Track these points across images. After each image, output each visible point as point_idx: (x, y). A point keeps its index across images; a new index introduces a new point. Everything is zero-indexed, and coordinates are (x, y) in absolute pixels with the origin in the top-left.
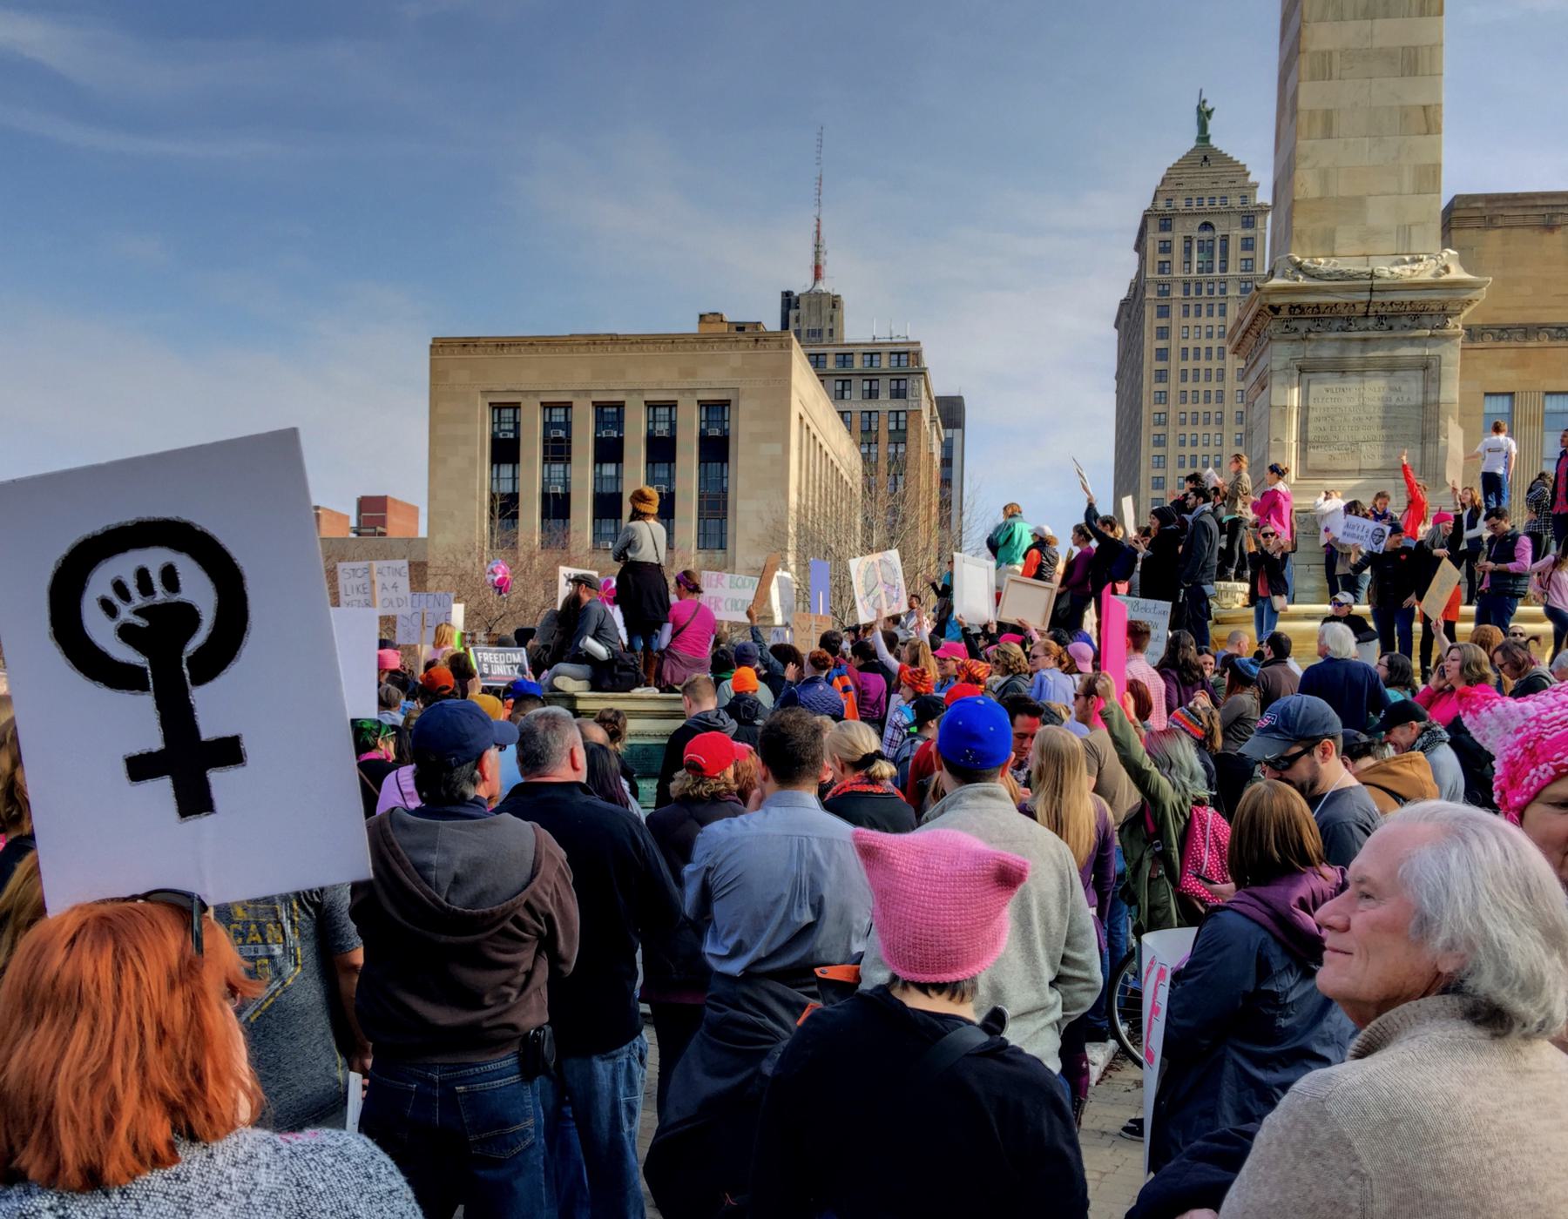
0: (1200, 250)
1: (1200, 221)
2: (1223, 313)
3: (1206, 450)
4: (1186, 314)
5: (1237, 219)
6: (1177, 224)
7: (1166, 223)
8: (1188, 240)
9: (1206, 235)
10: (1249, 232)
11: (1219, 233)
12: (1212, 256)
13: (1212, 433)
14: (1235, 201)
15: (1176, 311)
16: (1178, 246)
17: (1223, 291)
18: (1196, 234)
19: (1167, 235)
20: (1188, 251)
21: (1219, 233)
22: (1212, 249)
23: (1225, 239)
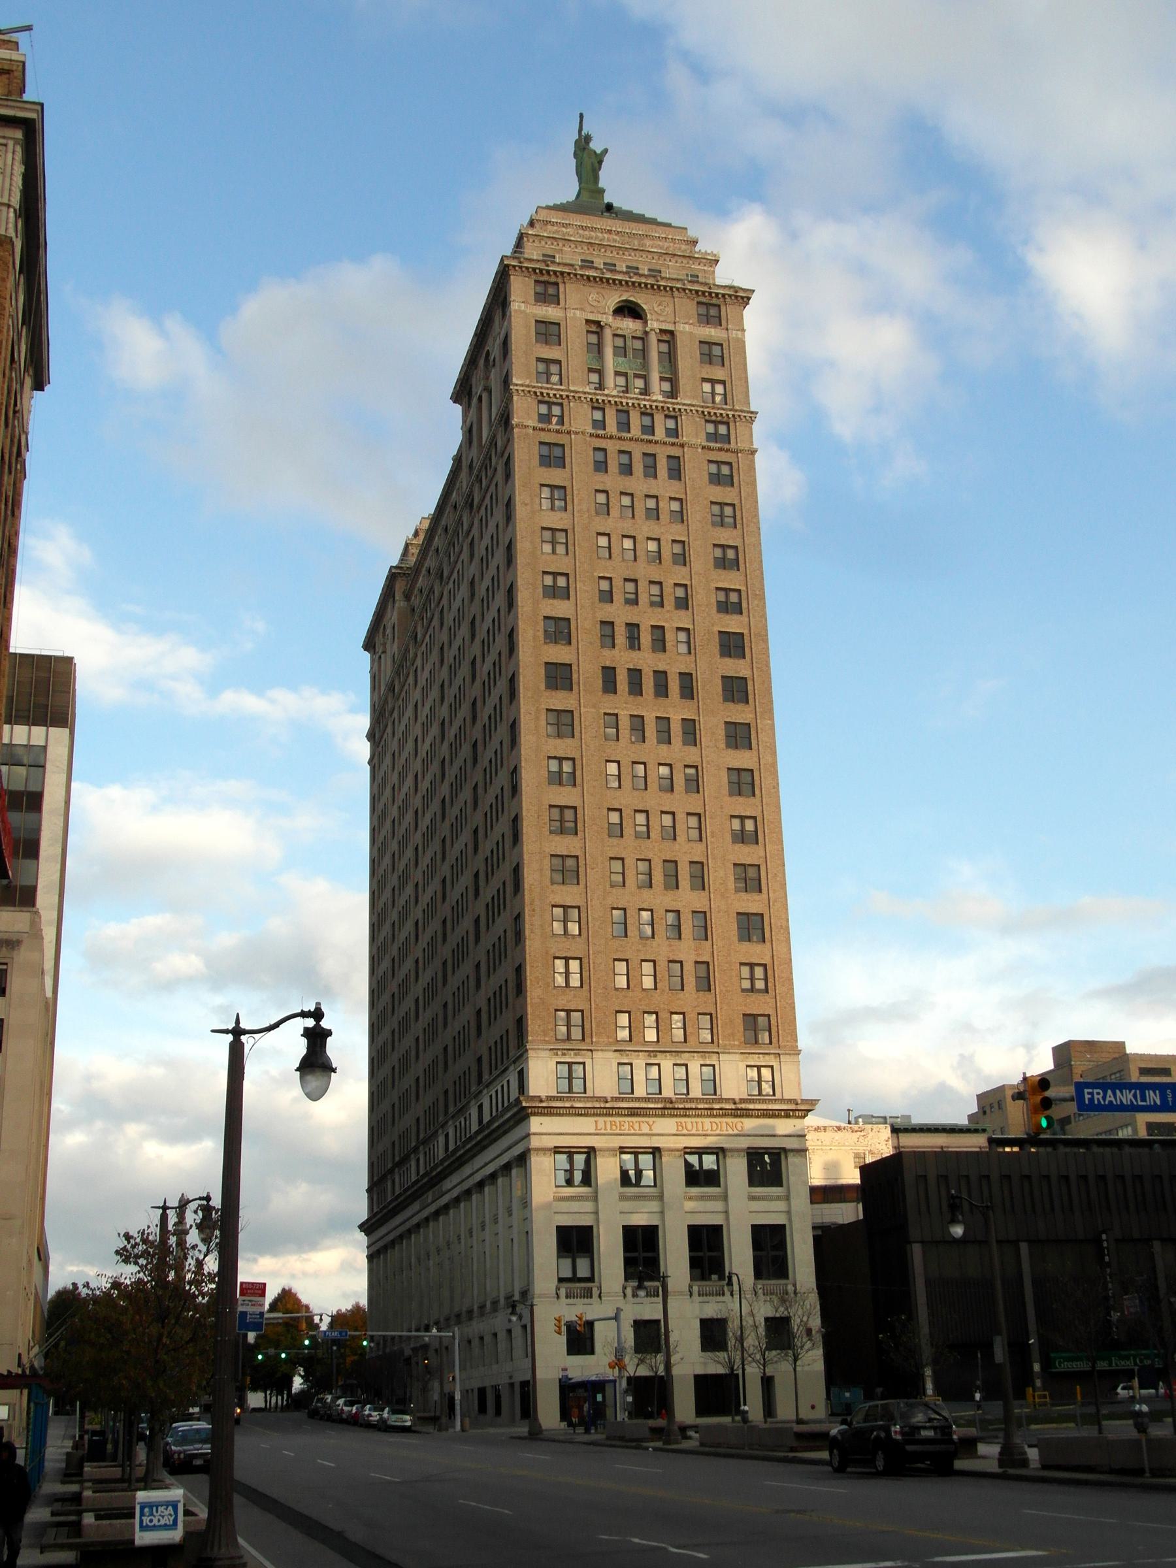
0: (621, 351)
1: (614, 298)
2: (676, 472)
4: (601, 466)
5: (688, 307)
6: (571, 293)
7: (548, 287)
8: (596, 328)
9: (629, 325)
10: (712, 333)
12: (645, 364)
17: (674, 433)
18: (607, 318)
19: (550, 312)
21: (653, 324)
22: (644, 353)
23: (669, 337)
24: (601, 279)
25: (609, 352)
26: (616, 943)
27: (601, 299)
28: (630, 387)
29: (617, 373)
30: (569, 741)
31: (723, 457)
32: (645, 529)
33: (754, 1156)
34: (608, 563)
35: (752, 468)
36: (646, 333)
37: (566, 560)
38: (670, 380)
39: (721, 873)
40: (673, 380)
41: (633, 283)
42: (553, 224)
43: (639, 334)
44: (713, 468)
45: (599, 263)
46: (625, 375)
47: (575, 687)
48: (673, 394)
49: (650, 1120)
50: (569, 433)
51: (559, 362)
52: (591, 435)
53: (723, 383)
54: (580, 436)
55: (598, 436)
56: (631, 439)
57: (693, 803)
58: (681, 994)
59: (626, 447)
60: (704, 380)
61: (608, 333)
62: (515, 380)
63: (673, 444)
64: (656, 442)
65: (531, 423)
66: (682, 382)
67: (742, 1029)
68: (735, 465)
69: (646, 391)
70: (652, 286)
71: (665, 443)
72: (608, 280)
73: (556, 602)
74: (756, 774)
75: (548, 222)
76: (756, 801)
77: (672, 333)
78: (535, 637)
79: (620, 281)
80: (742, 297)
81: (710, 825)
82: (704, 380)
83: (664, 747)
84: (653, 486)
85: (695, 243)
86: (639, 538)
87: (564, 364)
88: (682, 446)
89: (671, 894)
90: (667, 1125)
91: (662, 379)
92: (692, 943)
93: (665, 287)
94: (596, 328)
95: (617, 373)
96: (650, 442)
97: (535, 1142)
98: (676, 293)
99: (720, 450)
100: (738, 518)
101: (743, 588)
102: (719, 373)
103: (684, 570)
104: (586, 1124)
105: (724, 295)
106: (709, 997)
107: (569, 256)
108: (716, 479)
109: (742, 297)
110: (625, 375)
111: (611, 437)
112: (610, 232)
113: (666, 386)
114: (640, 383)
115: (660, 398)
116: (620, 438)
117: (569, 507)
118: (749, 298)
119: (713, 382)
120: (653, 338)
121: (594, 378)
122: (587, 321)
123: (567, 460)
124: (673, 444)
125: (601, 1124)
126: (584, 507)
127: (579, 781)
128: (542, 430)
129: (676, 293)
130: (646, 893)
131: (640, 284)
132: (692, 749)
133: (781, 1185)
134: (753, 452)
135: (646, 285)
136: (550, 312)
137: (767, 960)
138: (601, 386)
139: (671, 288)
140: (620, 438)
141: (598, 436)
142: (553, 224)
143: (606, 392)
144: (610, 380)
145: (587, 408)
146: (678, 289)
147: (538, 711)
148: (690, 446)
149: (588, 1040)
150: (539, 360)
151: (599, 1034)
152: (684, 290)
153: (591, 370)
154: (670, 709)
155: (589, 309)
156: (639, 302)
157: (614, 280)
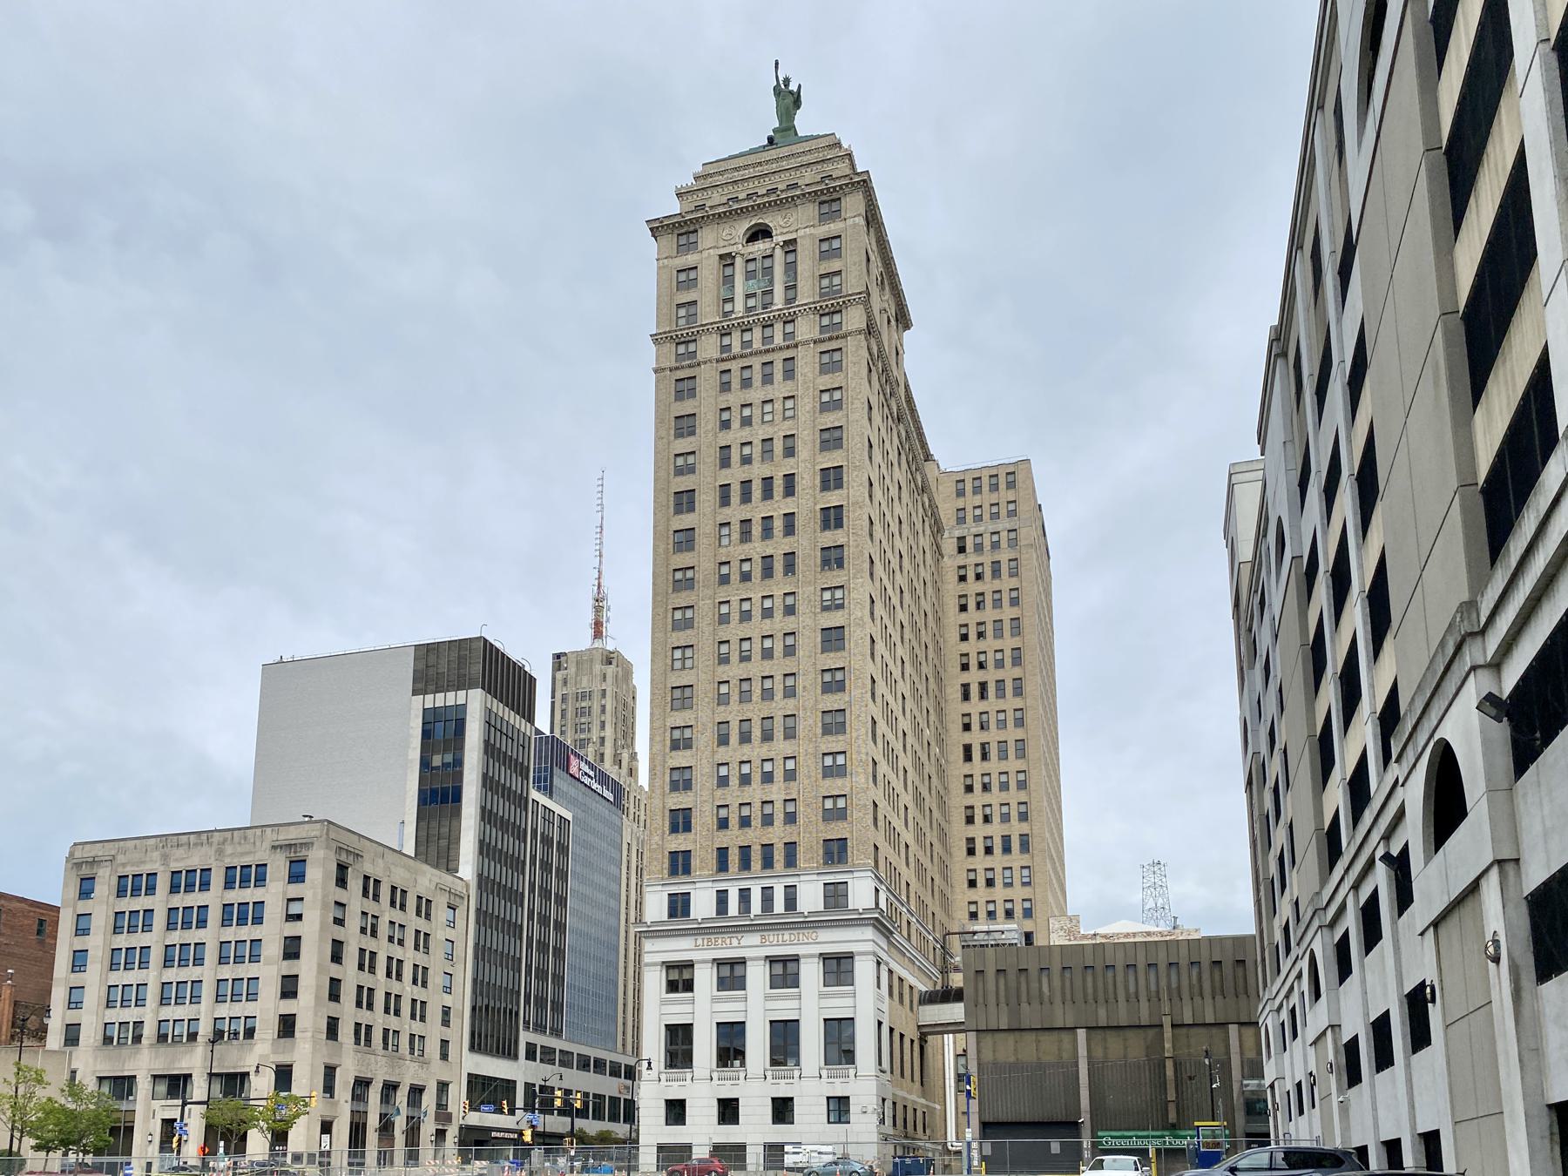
0: (750, 275)
1: (743, 226)
4: (725, 387)
8: (727, 260)
16: (709, 274)
20: (729, 280)
22: (769, 271)
26: (719, 792)
29: (748, 296)
46: (754, 295)
58: (770, 829)
61: (739, 261)
83: (768, 621)
92: (782, 784)
95: (748, 296)
96: (768, 351)
122: (721, 257)
125: (700, 942)
130: (746, 748)
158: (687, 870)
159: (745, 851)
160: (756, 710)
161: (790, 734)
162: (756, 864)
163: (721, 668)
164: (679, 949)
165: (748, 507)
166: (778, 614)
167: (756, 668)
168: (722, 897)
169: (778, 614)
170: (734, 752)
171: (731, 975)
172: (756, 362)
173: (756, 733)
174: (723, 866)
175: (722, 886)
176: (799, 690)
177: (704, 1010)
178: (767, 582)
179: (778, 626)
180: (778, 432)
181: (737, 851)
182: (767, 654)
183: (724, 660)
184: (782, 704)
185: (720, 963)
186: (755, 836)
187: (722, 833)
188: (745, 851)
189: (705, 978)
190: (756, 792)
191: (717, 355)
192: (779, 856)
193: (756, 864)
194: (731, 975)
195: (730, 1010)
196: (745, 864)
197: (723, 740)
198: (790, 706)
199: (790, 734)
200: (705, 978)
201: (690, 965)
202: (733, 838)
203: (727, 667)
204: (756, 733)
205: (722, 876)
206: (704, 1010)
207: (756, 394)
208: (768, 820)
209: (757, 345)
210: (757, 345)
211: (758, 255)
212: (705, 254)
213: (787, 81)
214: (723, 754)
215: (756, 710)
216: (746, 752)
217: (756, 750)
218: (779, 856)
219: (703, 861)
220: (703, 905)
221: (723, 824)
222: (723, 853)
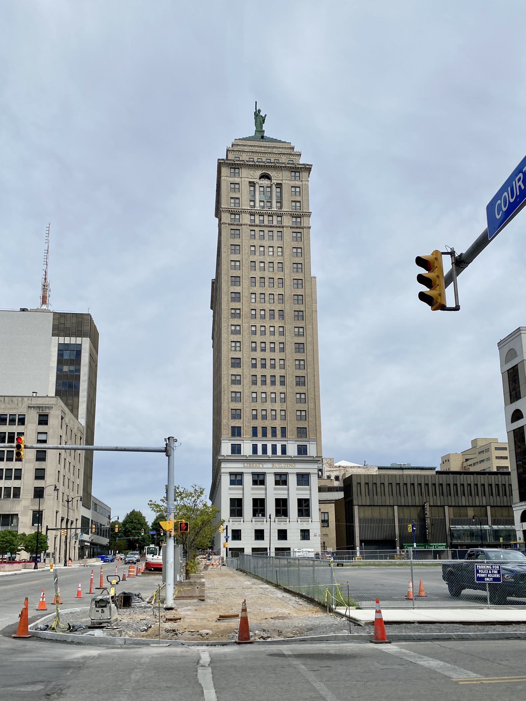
3: (272, 339)
8: (252, 184)
9: (265, 182)
11: (275, 182)
12: (271, 197)
13: (277, 326)
14: (284, 159)
15: (245, 231)
16: (245, 188)
23: (279, 186)
24: (255, 165)
25: (257, 193)
26: (253, 404)
27: (255, 174)
28: (265, 206)
29: (260, 201)
30: (238, 336)
31: (298, 230)
32: (268, 259)
33: (298, 475)
34: (254, 272)
35: (309, 234)
36: (272, 185)
37: (239, 272)
38: (280, 202)
39: (291, 380)
40: (281, 202)
41: (267, 166)
42: (240, 145)
43: (269, 185)
44: (295, 235)
45: (256, 160)
46: (263, 201)
47: (241, 317)
48: (281, 207)
49: (263, 463)
50: (241, 225)
51: (239, 198)
52: (249, 225)
53: (300, 202)
54: (245, 226)
55: (252, 226)
56: (264, 226)
57: (282, 355)
58: (275, 421)
59: (262, 229)
60: (292, 201)
61: (257, 186)
62: (222, 207)
63: (279, 227)
64: (273, 226)
65: (227, 222)
66: (284, 202)
67: (296, 432)
68: (302, 233)
69: (271, 207)
70: (274, 166)
71: (276, 227)
72: (257, 165)
73: (235, 287)
74: (305, 345)
75: (238, 145)
76: (305, 354)
77: (281, 184)
78: (228, 300)
79: (262, 165)
80: (308, 169)
81: (287, 363)
82: (292, 201)
83: (273, 336)
84: (271, 243)
85: (293, 148)
86: (266, 262)
87: (240, 199)
88: (283, 227)
89: (273, 387)
90: (270, 465)
91: (277, 202)
93: (279, 166)
94: (252, 184)
95: (260, 201)
96: (271, 226)
97: (223, 470)
98: (283, 169)
99: (297, 228)
100: (303, 252)
101: (303, 279)
102: (298, 199)
103: (282, 273)
104: (240, 465)
105: (301, 168)
106: (285, 422)
107: (245, 157)
108: (296, 239)
109: (308, 169)
110: (263, 201)
111: (257, 226)
112: (261, 147)
113: (279, 205)
114: (269, 204)
115: (276, 210)
116: (260, 226)
117: (241, 253)
118: (311, 168)
119: (296, 202)
120: (274, 187)
121: (252, 204)
123: (241, 235)
124: (279, 227)
126: (246, 252)
127: (242, 349)
128: (232, 224)
129: (283, 169)
130: (264, 387)
131: (269, 166)
132: (283, 337)
133: (309, 485)
134: (309, 228)
135: (271, 166)
136: (237, 180)
137: (306, 409)
138: (254, 206)
139: (281, 167)
140: (260, 226)
141: (252, 226)
142: (240, 145)
143: (256, 209)
144: (257, 205)
145: (248, 215)
146: (283, 167)
147: (228, 325)
148: (287, 227)
149: (242, 437)
150: (232, 198)
151: (246, 435)
152: (286, 167)
153: (251, 201)
154: (275, 323)
155: (250, 177)
156: (269, 173)
157: (259, 165)
158: (239, 435)
159: (264, 429)
160: (268, 372)
161: (283, 383)
162: (269, 435)
163: (253, 353)
164: (236, 467)
165: (264, 289)
166: (277, 334)
167: (268, 355)
168: (255, 448)
169: (277, 334)
170: (259, 388)
171: (259, 480)
172: (266, 230)
173: (268, 381)
174: (255, 434)
175: (255, 443)
176: (287, 366)
177: (249, 493)
178: (272, 320)
179: (277, 339)
180: (276, 260)
181: (261, 429)
182: (273, 350)
183: (254, 350)
184: (279, 371)
185: (253, 474)
186: (269, 424)
187: (254, 421)
188: (264, 429)
189: (248, 480)
190: (268, 406)
191: (249, 223)
192: (279, 432)
193: (269, 435)
194: (259, 480)
195: (259, 493)
196: (264, 434)
197: (254, 383)
198: (282, 372)
199: (283, 383)
200: (248, 480)
201: (241, 474)
202: (259, 423)
203: (255, 353)
204: (268, 381)
205: (255, 438)
206: (249, 493)
207: (266, 243)
208: (275, 418)
209: (266, 223)
210: (266, 223)
211: (265, 186)
212: (243, 179)
213: (259, 111)
214: (254, 388)
215: (268, 372)
216: (264, 388)
217: (268, 388)
218: (279, 432)
219: (247, 431)
220: (247, 449)
221: (255, 417)
222: (255, 429)
